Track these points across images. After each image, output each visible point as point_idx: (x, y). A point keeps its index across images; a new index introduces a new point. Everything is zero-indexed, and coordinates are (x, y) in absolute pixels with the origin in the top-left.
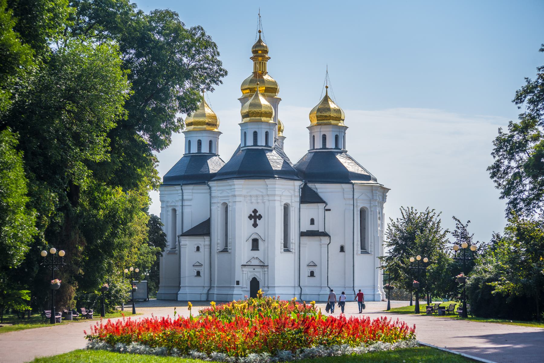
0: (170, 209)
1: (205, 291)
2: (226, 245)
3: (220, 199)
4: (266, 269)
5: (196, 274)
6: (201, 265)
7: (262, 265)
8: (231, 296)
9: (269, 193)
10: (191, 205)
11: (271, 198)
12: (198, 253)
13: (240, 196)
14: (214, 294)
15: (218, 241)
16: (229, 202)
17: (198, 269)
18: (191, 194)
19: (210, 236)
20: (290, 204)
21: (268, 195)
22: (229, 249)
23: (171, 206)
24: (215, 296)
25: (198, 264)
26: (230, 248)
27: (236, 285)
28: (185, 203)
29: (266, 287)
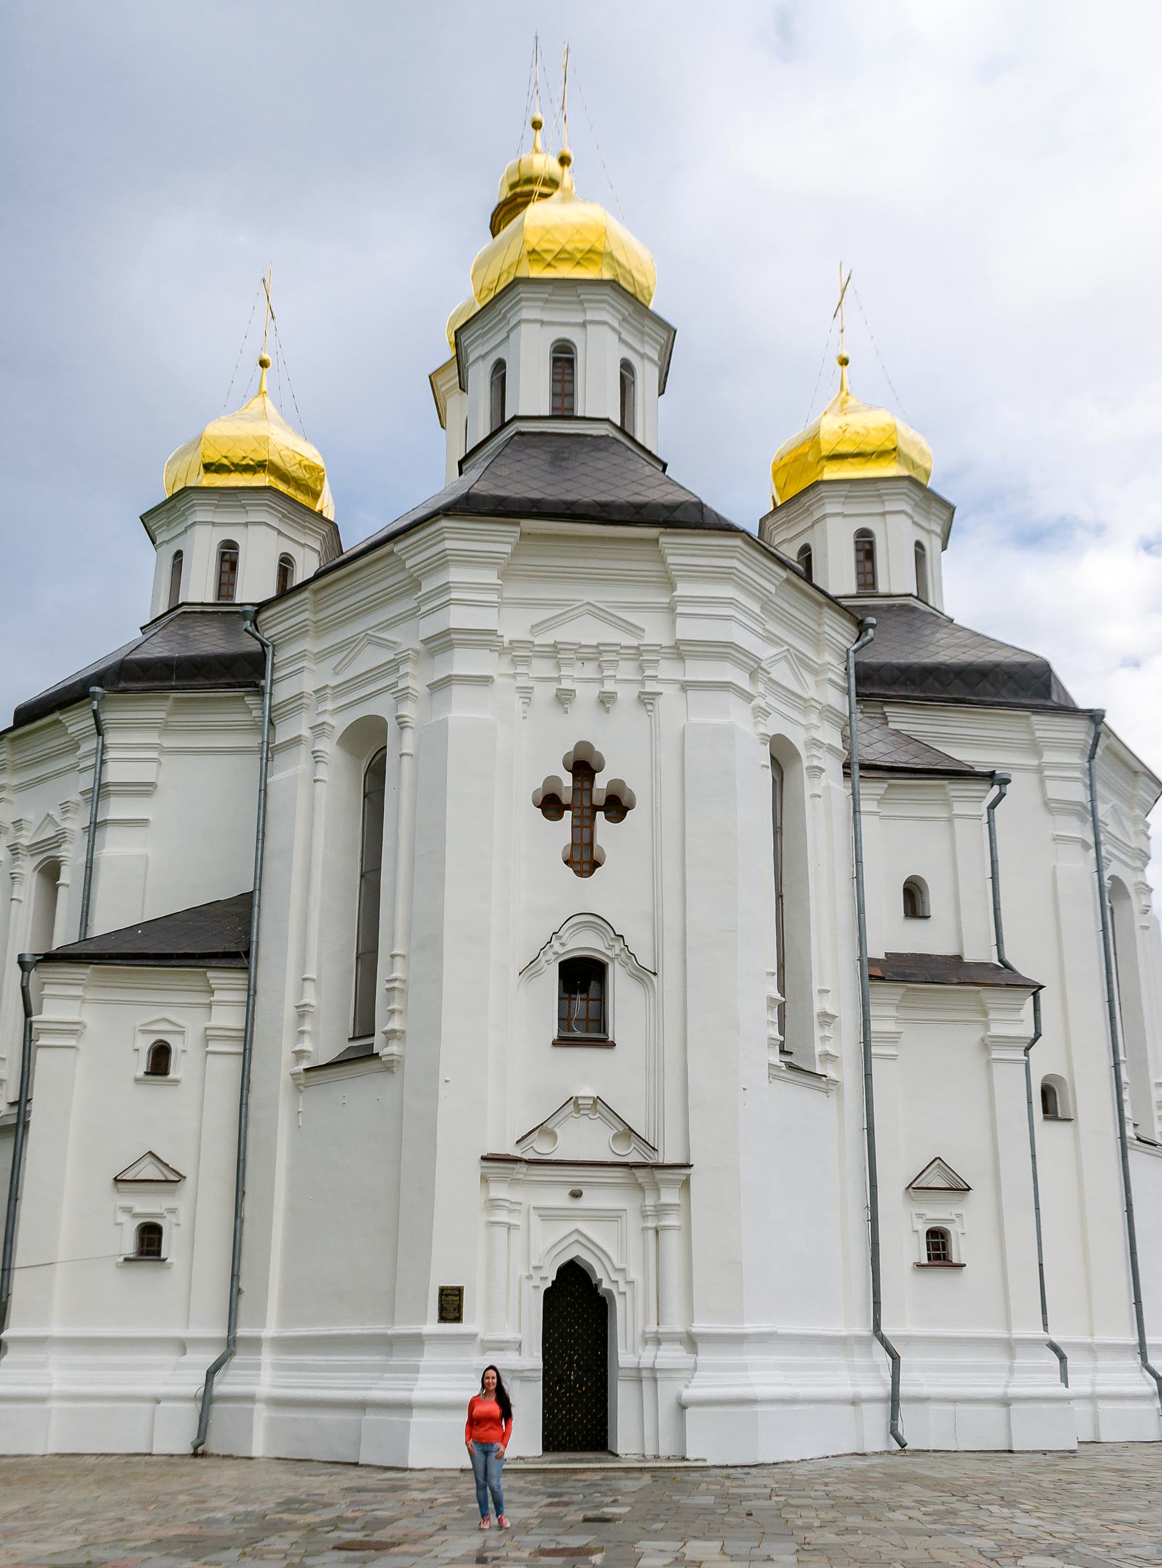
0: (28, 867)
1: (194, 1383)
2: (365, 1024)
3: (330, 705)
4: (670, 1196)
5: (129, 1244)
6: (172, 1180)
7: (634, 1158)
8: (395, 1418)
9: (687, 630)
10: (143, 822)
11: (698, 671)
12: (157, 1091)
13: (484, 639)
14: (250, 1398)
15: (301, 992)
16: (403, 695)
17: (149, 1206)
18: (154, 755)
19: (246, 969)
20: (803, 753)
21: (680, 651)
22: (391, 1035)
23: (35, 848)
24: (261, 1413)
25: (150, 1171)
26: (395, 1024)
27: (432, 1326)
28: (115, 809)
29: (673, 1338)
